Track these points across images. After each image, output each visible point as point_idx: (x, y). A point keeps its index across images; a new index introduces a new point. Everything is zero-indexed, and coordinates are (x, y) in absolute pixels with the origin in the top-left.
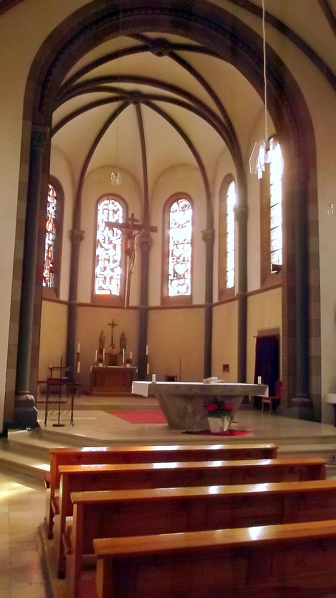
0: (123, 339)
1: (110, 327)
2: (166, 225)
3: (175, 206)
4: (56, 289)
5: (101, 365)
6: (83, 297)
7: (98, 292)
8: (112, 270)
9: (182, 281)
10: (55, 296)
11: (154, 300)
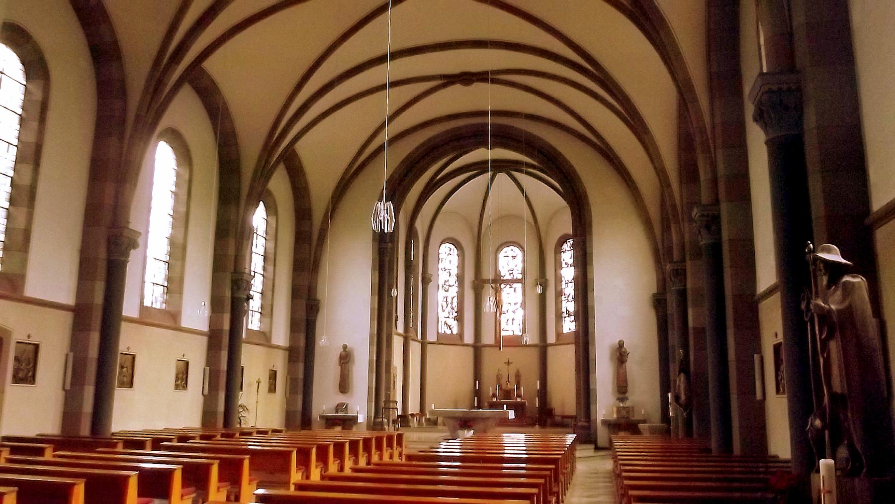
0: (518, 376)
1: (506, 366)
2: (558, 265)
4: (461, 335)
6: (488, 338)
8: (514, 312)
11: (551, 338)
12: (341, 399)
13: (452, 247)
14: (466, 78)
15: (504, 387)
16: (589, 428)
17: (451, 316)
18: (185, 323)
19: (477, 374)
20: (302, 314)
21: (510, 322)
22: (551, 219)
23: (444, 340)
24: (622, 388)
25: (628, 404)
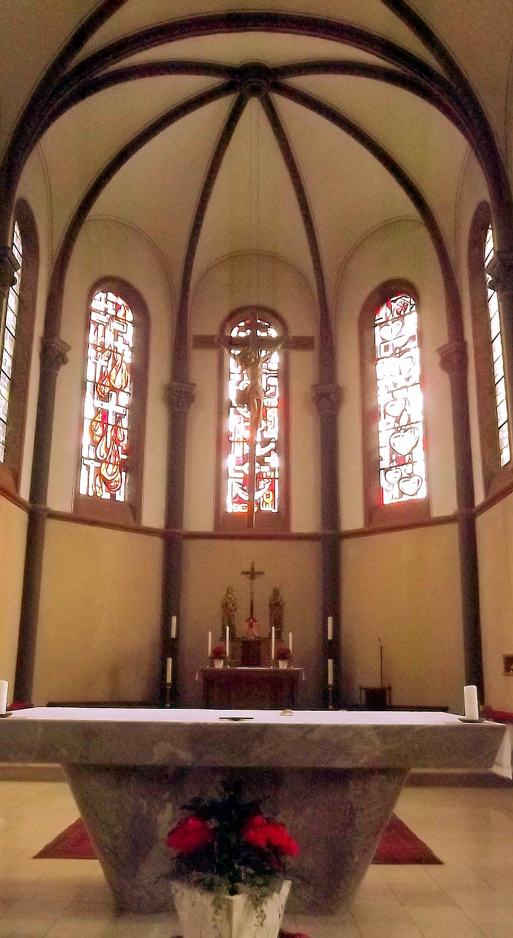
0: (276, 606)
1: (246, 580)
2: (368, 352)
3: (384, 312)
4: (134, 506)
5: (219, 665)
6: (198, 518)
7: (232, 508)
9: (408, 468)
10: (131, 519)
11: (352, 517)
15: (239, 635)
22: (348, 258)
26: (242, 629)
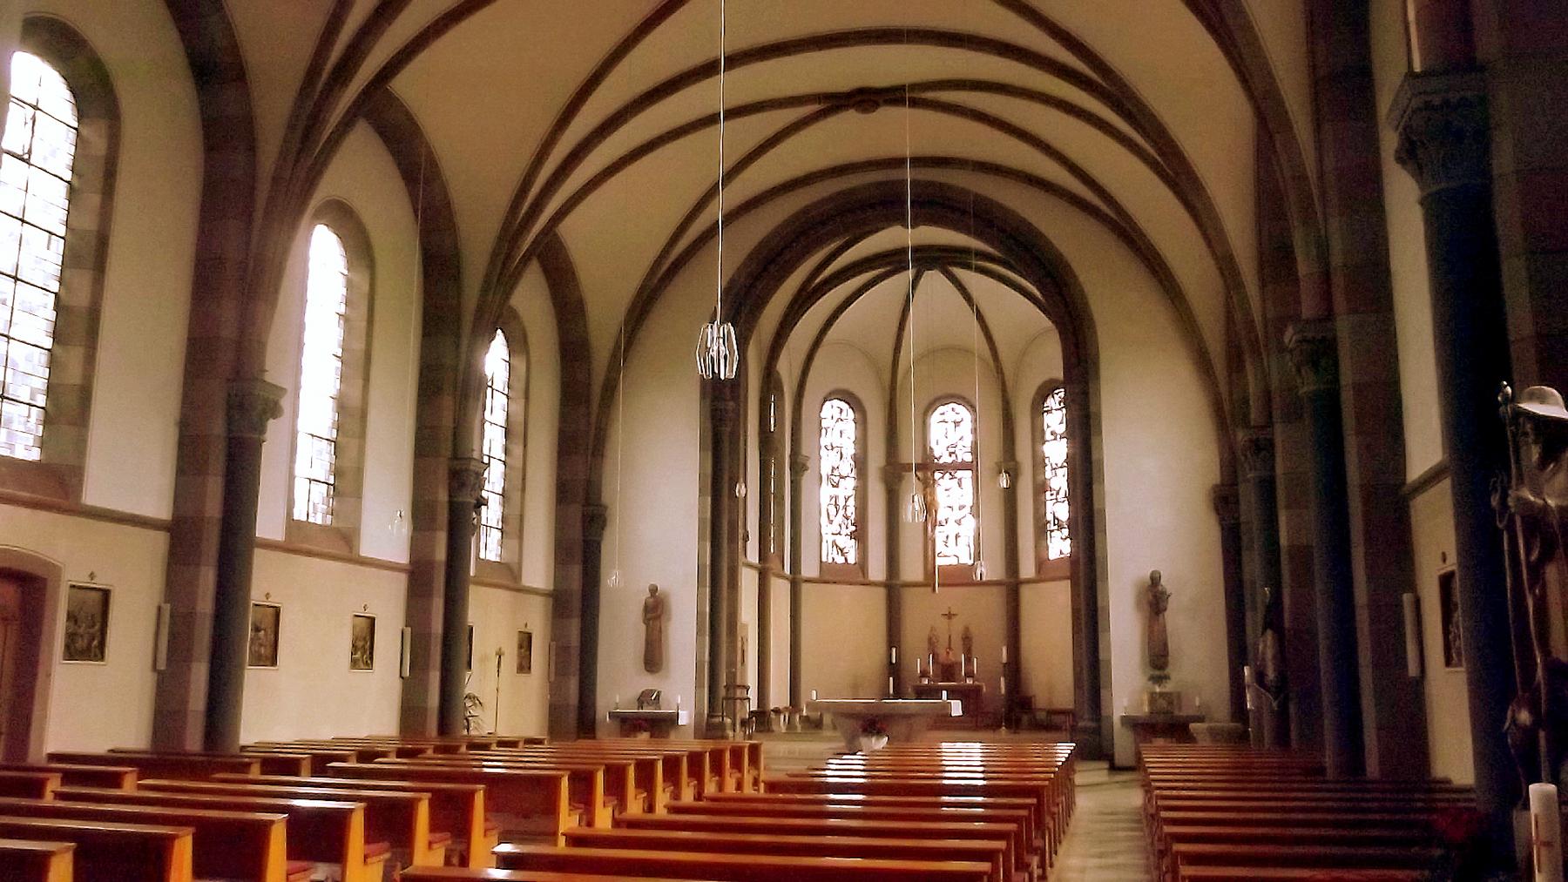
0: (967, 639)
1: (945, 620)
6: (912, 570)
8: (959, 522)
11: (1027, 569)
12: (648, 682)
13: (844, 406)
14: (866, 99)
16: (1097, 731)
17: (844, 531)
18: (367, 549)
19: (893, 636)
20: (576, 533)
21: (952, 540)
22: (1024, 353)
23: (831, 575)
24: (1158, 658)
25: (1169, 687)
26: (942, 658)
